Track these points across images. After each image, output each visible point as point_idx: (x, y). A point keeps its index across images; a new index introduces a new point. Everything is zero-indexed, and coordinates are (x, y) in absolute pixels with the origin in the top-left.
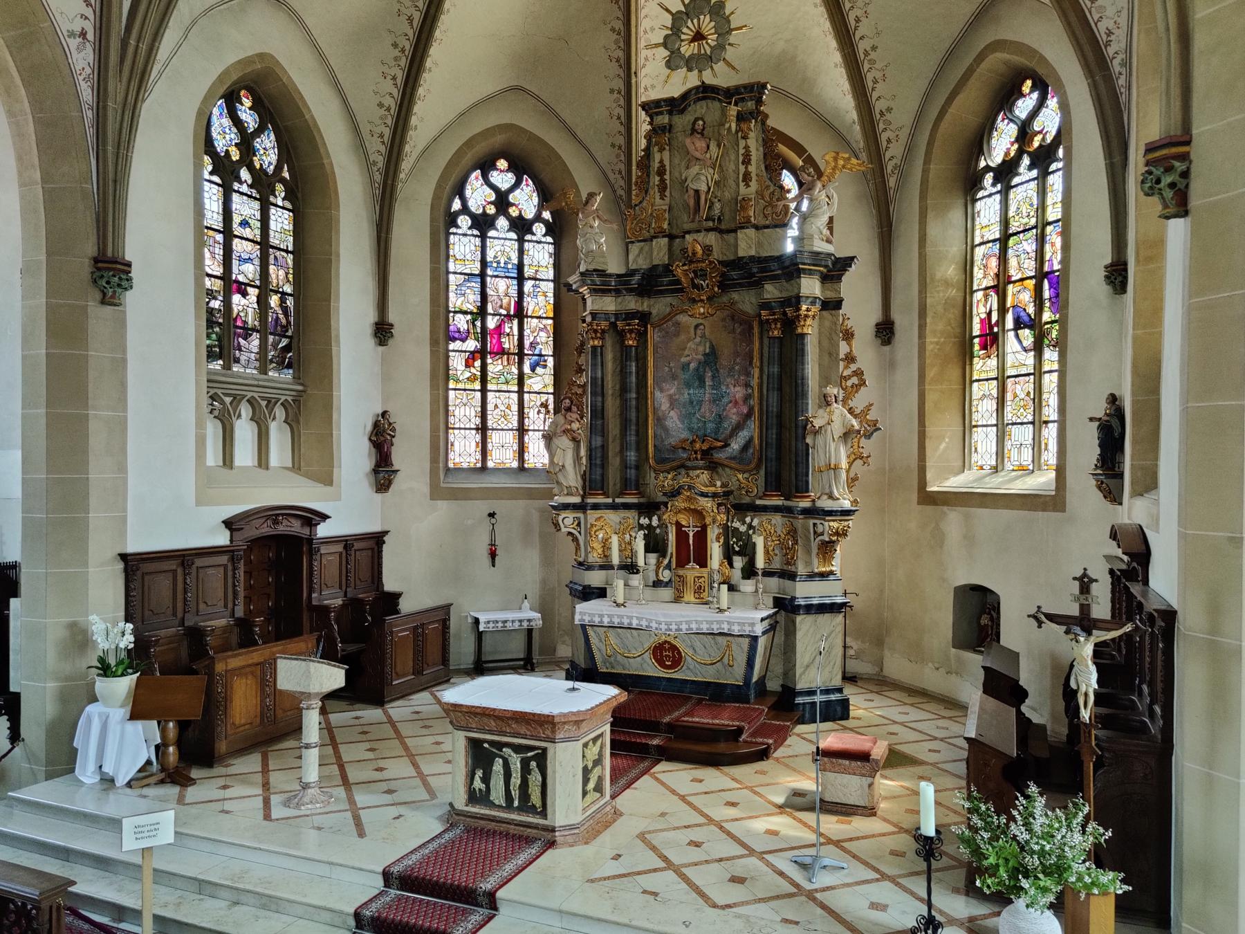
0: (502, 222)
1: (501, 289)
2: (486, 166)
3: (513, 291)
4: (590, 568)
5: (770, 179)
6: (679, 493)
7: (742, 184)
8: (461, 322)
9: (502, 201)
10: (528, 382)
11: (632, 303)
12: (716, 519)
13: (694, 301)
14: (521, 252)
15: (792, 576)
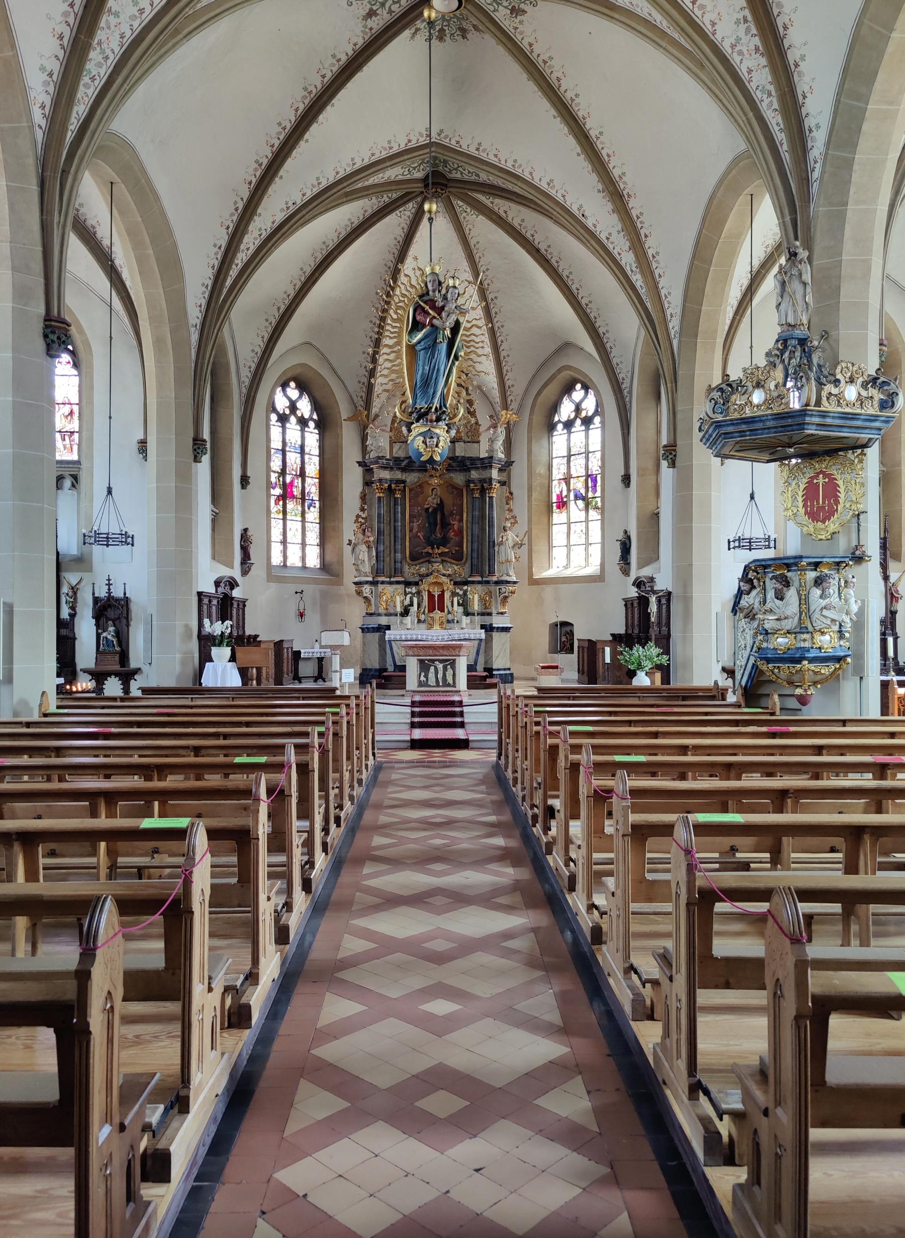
0: (293, 419)
1: (293, 459)
2: (284, 386)
3: (299, 461)
4: (379, 615)
6: (431, 574)
8: (273, 477)
9: (293, 407)
10: (307, 516)
11: (399, 475)
12: (449, 586)
14: (303, 438)
15: (490, 614)
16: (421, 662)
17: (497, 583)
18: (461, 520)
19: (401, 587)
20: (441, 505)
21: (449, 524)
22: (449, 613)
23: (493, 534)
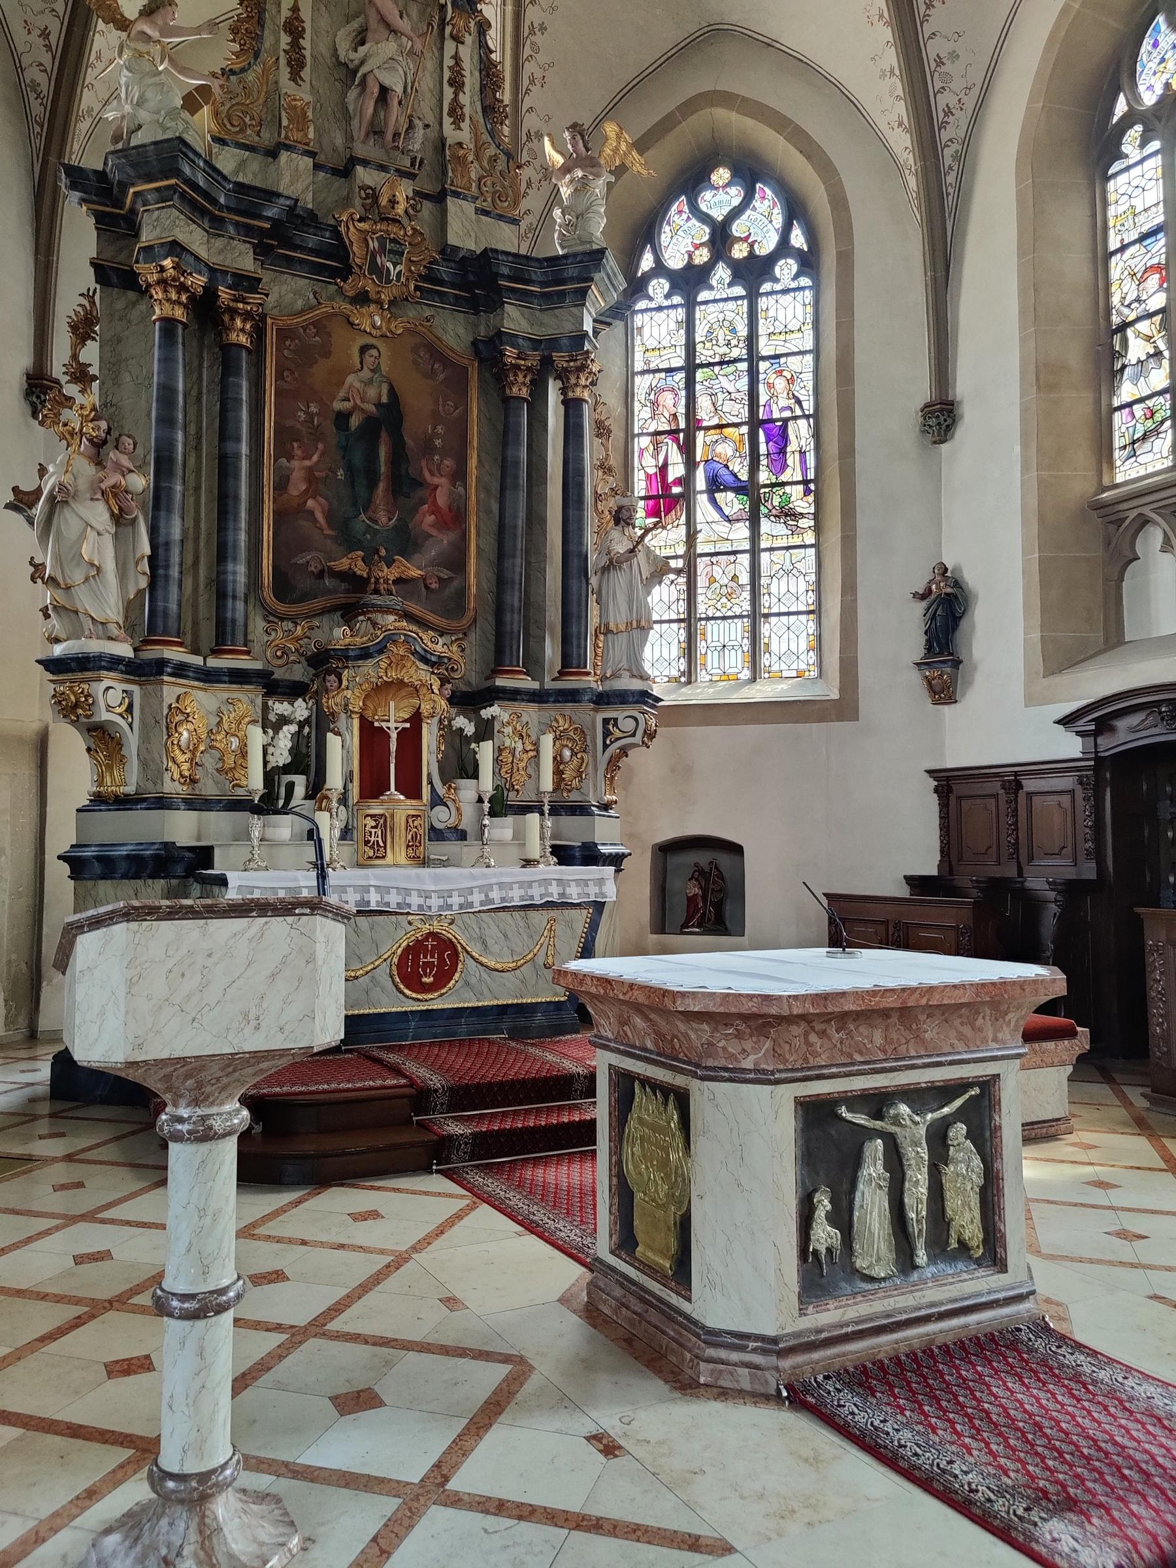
5: (492, 134)
7: (447, 121)
12: (435, 703)
13: (362, 299)
16: (816, 1115)
17: (603, 699)
18: (459, 475)
19: (247, 699)
20: (391, 413)
21: (419, 483)
22: (437, 801)
23: (581, 530)
